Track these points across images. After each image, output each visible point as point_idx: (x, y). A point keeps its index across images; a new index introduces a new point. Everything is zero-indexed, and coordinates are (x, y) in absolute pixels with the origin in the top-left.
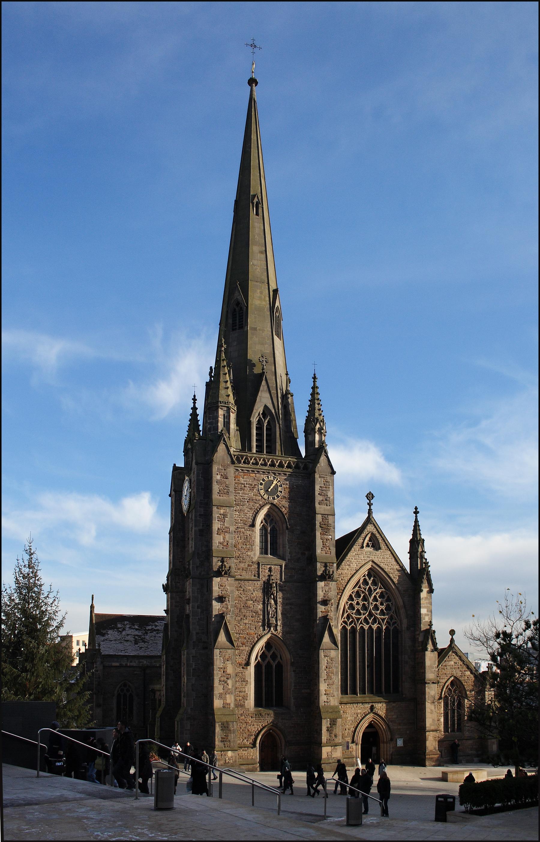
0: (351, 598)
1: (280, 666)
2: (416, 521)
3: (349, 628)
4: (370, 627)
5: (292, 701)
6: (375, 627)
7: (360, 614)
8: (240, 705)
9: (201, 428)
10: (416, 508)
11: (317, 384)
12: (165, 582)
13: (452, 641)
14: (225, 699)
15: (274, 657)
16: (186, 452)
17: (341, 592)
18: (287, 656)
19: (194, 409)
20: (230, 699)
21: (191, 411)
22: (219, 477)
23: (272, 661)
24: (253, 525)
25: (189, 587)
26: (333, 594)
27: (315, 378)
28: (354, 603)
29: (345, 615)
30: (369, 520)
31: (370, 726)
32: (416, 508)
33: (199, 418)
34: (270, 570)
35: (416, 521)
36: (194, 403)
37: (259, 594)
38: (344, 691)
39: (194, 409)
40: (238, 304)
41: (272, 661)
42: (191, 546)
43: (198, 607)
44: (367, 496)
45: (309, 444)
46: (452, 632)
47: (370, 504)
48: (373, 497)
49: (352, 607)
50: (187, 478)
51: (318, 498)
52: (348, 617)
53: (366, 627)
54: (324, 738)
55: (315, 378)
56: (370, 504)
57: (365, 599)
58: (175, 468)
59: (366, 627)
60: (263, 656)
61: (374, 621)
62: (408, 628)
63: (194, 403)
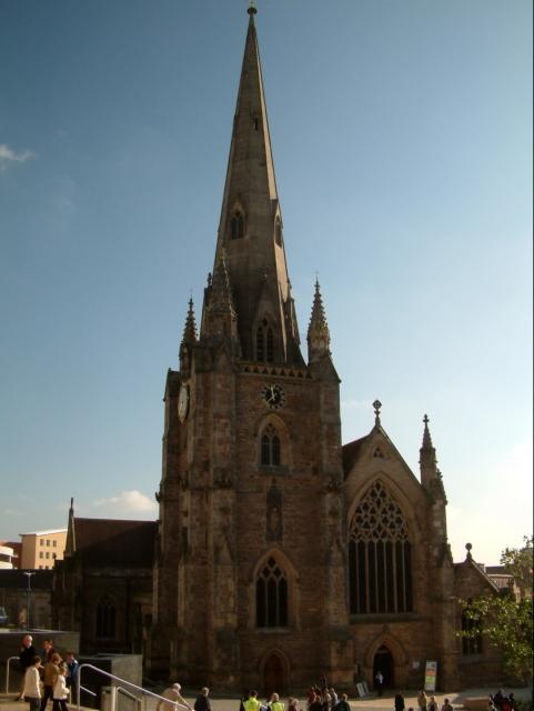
0: (358, 511)
1: (283, 583)
2: (427, 430)
3: (357, 541)
4: (380, 541)
5: (298, 620)
6: (385, 541)
7: (368, 527)
8: (242, 624)
9: (198, 332)
10: (426, 416)
11: (320, 292)
12: (158, 491)
13: (469, 556)
14: (226, 618)
15: (277, 572)
16: (182, 356)
17: (347, 504)
18: (291, 572)
19: (191, 313)
20: (232, 620)
21: (187, 315)
22: (219, 386)
23: (275, 578)
24: (256, 435)
25: (187, 501)
26: (340, 505)
27: (317, 286)
28: (363, 515)
29: (353, 528)
30: (377, 429)
31: (383, 647)
32: (426, 416)
33: (195, 322)
34: (274, 481)
35: (427, 430)
36: (191, 307)
37: (263, 506)
38: (353, 610)
39: (191, 313)
40: (238, 213)
41: (275, 578)
42: (189, 455)
43: (197, 520)
44: (374, 404)
45: (311, 352)
46: (469, 546)
47: (377, 413)
48: (380, 405)
49: (359, 520)
50: (184, 384)
51: (323, 407)
52: (356, 530)
53: (376, 541)
54: (334, 661)
55: (317, 286)
56: (377, 413)
57: (373, 511)
58: (171, 373)
59: (376, 541)
60: (266, 572)
61: (384, 535)
62: (422, 541)
63: (191, 307)
